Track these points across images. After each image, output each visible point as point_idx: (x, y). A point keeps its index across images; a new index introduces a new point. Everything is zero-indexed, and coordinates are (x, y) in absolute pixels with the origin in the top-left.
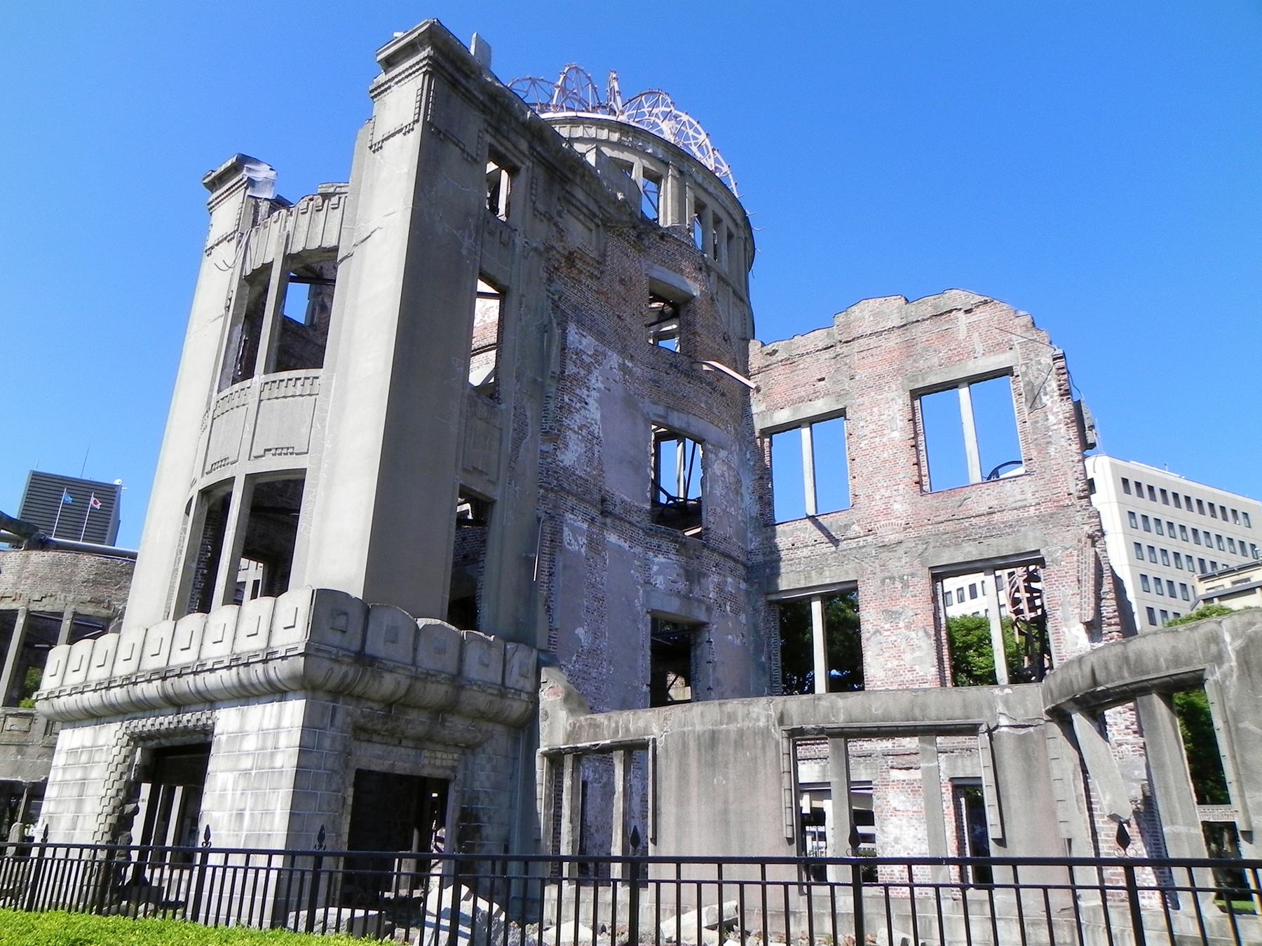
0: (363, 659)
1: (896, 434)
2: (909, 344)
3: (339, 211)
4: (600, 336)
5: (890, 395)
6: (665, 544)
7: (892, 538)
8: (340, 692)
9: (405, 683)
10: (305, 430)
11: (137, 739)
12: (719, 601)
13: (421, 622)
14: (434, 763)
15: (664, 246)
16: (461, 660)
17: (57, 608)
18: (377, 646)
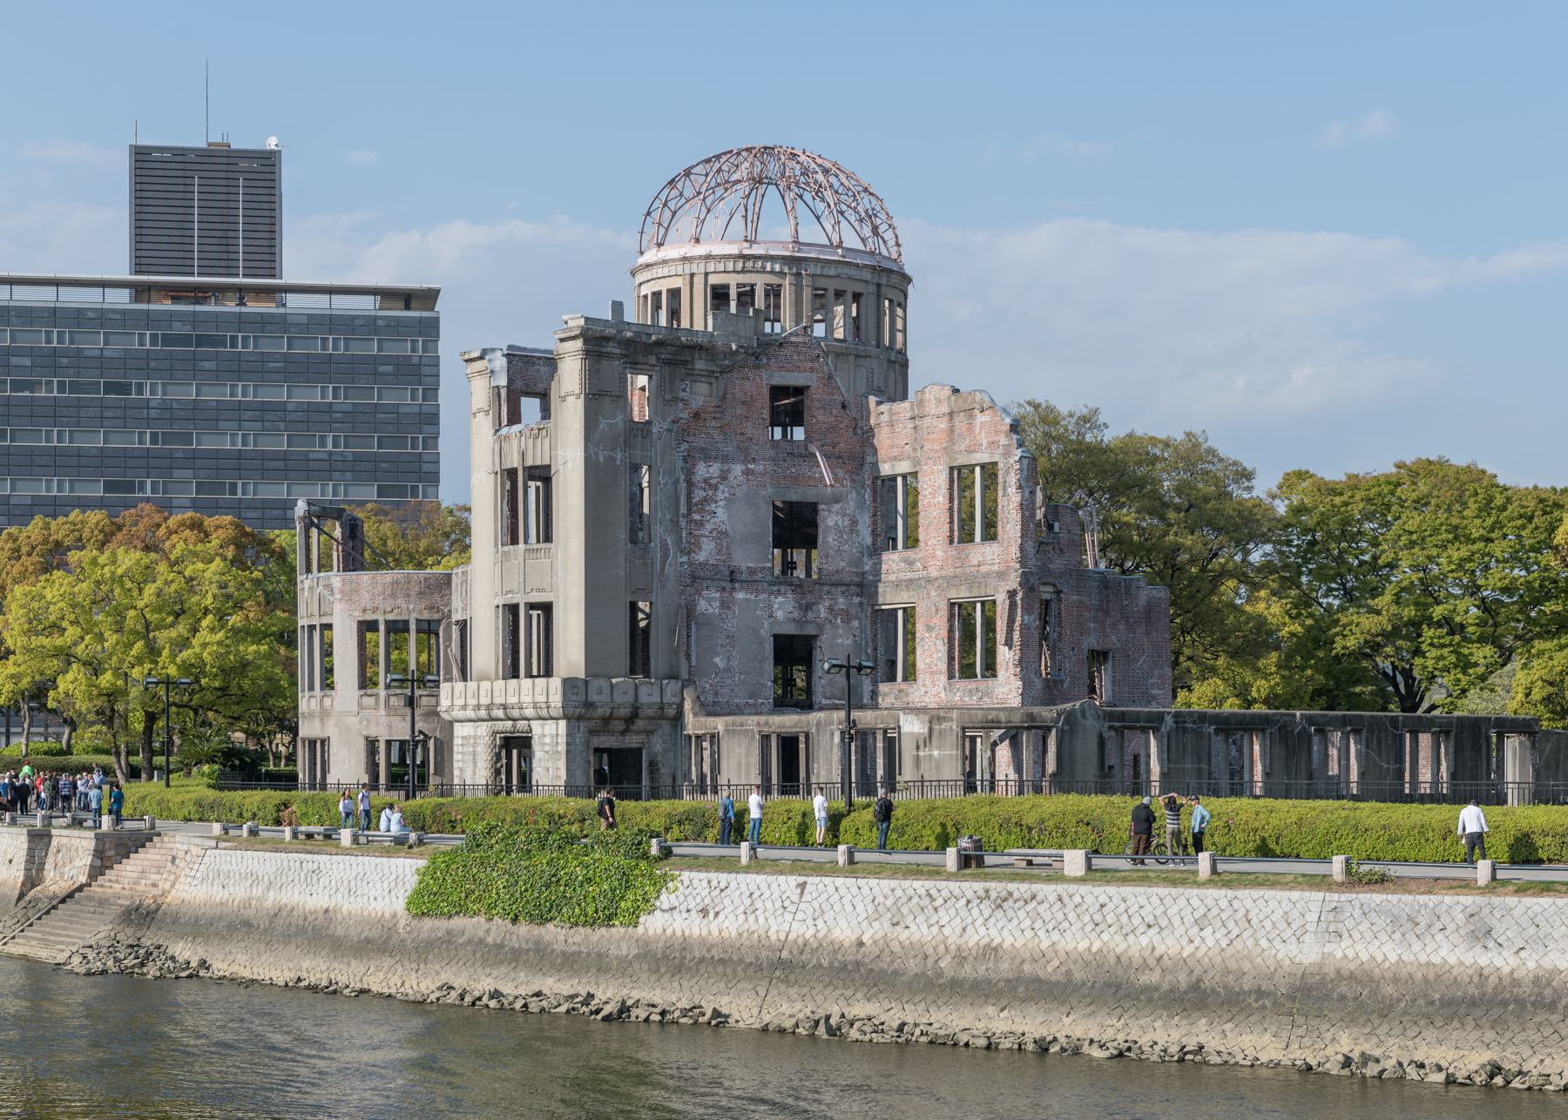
0: (588, 705)
1: (941, 499)
2: (952, 431)
3: (548, 440)
4: (725, 459)
5: (941, 468)
6: (783, 589)
7: (934, 573)
8: (579, 718)
9: (609, 711)
10: (549, 579)
11: (495, 733)
12: (830, 617)
13: (614, 681)
14: (632, 741)
15: (785, 351)
16: (636, 695)
17: (404, 617)
18: (593, 697)
